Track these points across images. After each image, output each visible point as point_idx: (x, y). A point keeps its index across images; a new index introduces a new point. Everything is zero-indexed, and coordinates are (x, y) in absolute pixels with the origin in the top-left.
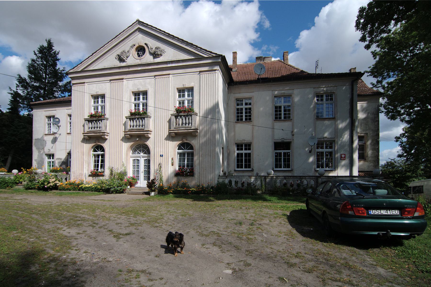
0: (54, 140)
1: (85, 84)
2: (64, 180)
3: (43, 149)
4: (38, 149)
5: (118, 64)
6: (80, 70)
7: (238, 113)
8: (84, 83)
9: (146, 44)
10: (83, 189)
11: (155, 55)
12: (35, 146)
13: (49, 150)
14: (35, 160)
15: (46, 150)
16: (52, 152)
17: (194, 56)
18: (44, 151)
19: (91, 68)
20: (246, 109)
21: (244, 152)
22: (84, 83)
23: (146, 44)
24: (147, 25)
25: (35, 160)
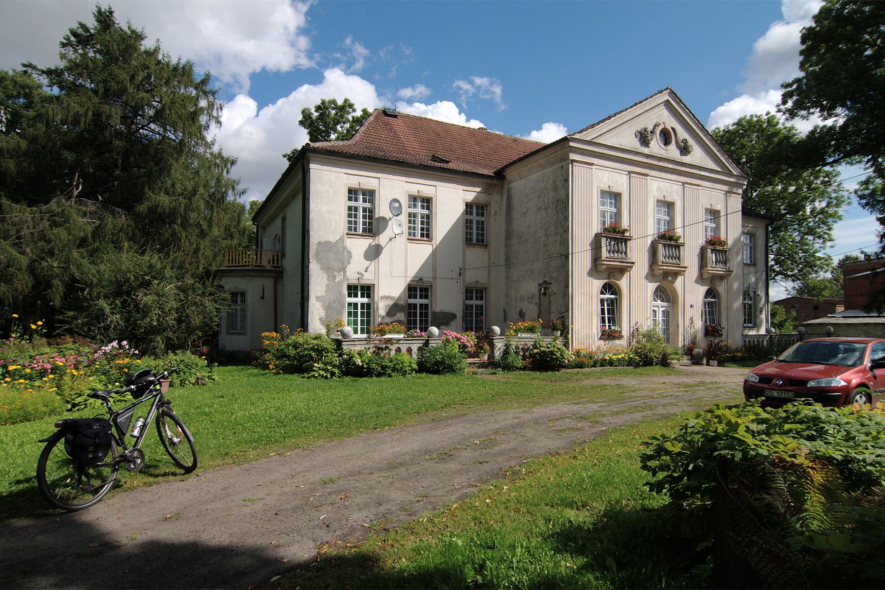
0: (374, 253)
1: (593, 167)
2: (404, 350)
3: (344, 270)
4: (328, 269)
5: (634, 144)
6: (588, 139)
7: (350, 216)
8: (592, 164)
9: (673, 129)
10: (611, 363)
11: (685, 149)
12: (319, 261)
13: (358, 273)
14: (318, 298)
15: (352, 276)
16: (368, 279)
17: (721, 168)
18: (345, 276)
19: (712, 165)
20: (478, 222)
21: (474, 302)
22: (592, 164)
23: (673, 129)
24: (679, 101)
25: (318, 298)
